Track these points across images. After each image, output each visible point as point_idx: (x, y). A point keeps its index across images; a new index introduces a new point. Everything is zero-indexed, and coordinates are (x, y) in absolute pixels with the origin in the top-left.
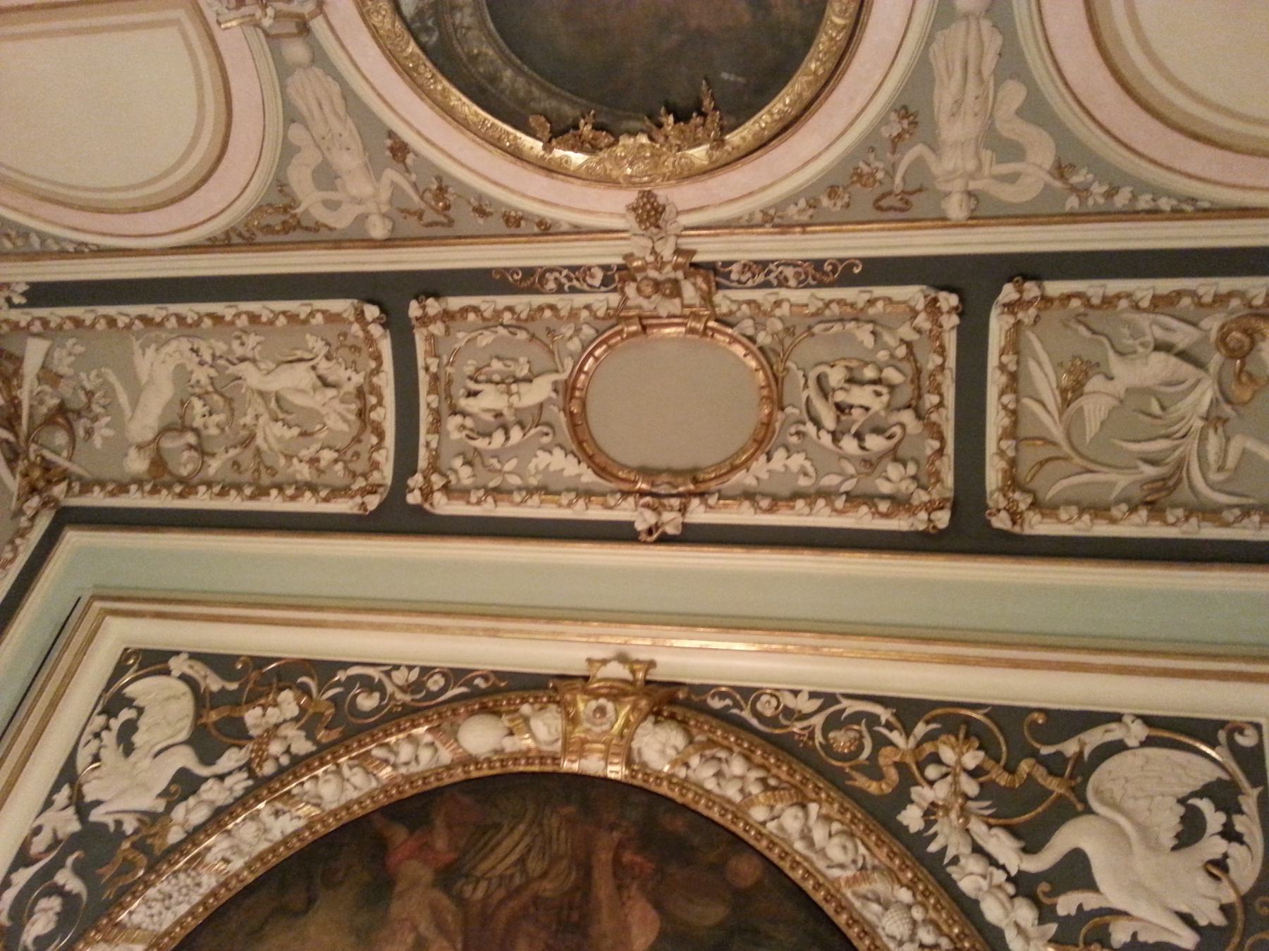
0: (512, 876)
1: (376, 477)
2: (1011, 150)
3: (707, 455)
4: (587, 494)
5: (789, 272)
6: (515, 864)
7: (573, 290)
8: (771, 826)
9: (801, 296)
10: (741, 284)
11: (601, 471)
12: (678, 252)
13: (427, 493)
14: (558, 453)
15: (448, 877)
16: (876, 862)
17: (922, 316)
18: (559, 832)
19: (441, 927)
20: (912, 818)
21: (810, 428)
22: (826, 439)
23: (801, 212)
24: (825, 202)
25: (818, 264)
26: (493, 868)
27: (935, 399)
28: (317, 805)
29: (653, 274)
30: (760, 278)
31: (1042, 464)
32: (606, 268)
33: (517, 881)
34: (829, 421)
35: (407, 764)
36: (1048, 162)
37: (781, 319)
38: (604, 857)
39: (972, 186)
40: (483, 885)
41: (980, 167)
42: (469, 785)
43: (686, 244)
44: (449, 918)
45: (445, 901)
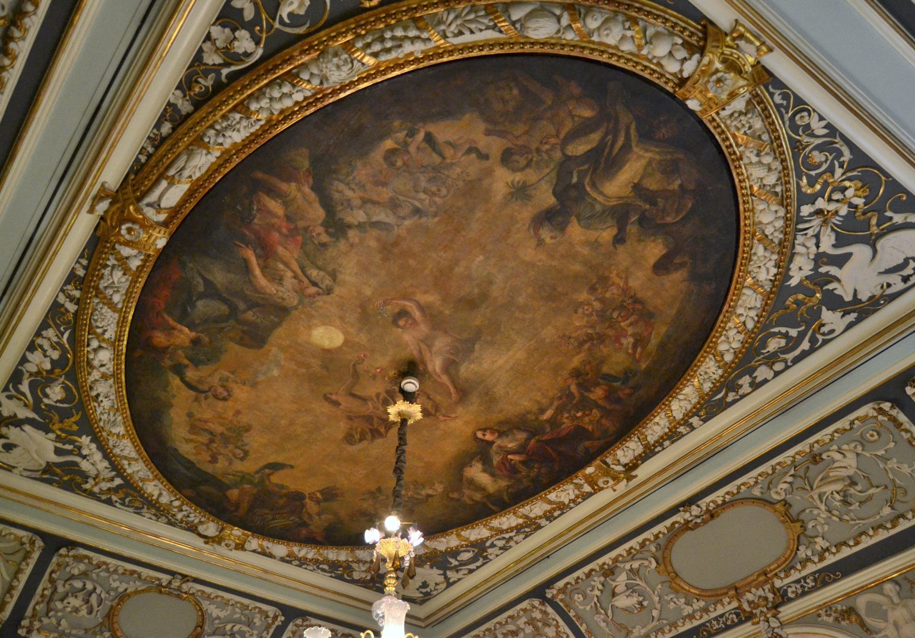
1: (295, 628)
3: (154, 595)
4: (208, 597)
8: (173, 499)
11: (198, 603)
13: (275, 617)
17: (36, 628)
20: (118, 481)
21: (103, 596)
22: (98, 591)
27: (46, 592)
31: (13, 554)
34: (94, 599)
42: (289, 540)
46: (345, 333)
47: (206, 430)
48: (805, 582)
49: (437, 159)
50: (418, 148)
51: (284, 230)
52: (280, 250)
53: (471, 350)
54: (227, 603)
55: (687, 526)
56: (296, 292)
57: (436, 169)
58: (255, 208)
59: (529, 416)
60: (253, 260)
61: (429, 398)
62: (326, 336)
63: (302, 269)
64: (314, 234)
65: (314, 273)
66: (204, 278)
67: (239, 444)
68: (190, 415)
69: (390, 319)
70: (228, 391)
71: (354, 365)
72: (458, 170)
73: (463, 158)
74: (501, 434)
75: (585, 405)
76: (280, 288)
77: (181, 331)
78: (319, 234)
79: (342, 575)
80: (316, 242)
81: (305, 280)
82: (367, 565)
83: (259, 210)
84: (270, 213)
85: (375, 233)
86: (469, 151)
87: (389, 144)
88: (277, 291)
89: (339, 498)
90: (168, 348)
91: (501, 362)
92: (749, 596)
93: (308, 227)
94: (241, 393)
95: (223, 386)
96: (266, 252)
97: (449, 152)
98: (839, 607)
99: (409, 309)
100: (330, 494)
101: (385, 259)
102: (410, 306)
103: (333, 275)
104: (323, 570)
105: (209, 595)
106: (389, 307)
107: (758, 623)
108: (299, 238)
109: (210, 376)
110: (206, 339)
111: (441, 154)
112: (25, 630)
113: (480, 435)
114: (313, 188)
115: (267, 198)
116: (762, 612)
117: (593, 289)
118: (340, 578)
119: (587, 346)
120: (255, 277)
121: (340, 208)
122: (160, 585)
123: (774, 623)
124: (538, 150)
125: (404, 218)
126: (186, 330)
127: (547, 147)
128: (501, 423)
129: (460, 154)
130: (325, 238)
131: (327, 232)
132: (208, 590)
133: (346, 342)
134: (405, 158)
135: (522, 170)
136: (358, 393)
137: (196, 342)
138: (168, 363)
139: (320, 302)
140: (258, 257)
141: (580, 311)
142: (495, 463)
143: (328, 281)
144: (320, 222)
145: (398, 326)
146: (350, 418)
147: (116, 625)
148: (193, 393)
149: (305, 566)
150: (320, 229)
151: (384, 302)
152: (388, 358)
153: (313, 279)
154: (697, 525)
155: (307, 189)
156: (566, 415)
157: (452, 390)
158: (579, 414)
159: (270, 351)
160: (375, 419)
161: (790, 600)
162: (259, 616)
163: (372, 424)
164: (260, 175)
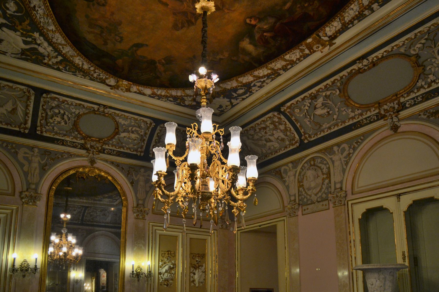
2: (26, 158)
5: (69, 144)
7: (111, 150)
9: (67, 139)
10: (79, 143)
12: (89, 153)
13: (151, 124)
14: (122, 124)
23: (64, 155)
24: (60, 156)
25: (63, 144)
29: (95, 151)
30: (75, 144)
32: (104, 153)
36: (19, 154)
37: (72, 136)
39: (33, 153)
41: (32, 157)
43: (87, 154)
48: (417, 99)
54: (127, 118)
55: (359, 71)
74: (260, 20)
79: (180, 103)
82: (192, 98)
92: (385, 107)
98: (432, 111)
104: (170, 101)
105: (118, 114)
107: (387, 120)
112: (40, 132)
113: (248, 21)
116: (390, 114)
118: (179, 104)
122: (94, 110)
123: (395, 119)
132: (117, 112)
142: (256, 38)
147: (79, 129)
149: (161, 99)
154: (365, 70)
156: (299, 6)
158: (306, 5)
161: (407, 108)
162: (143, 123)
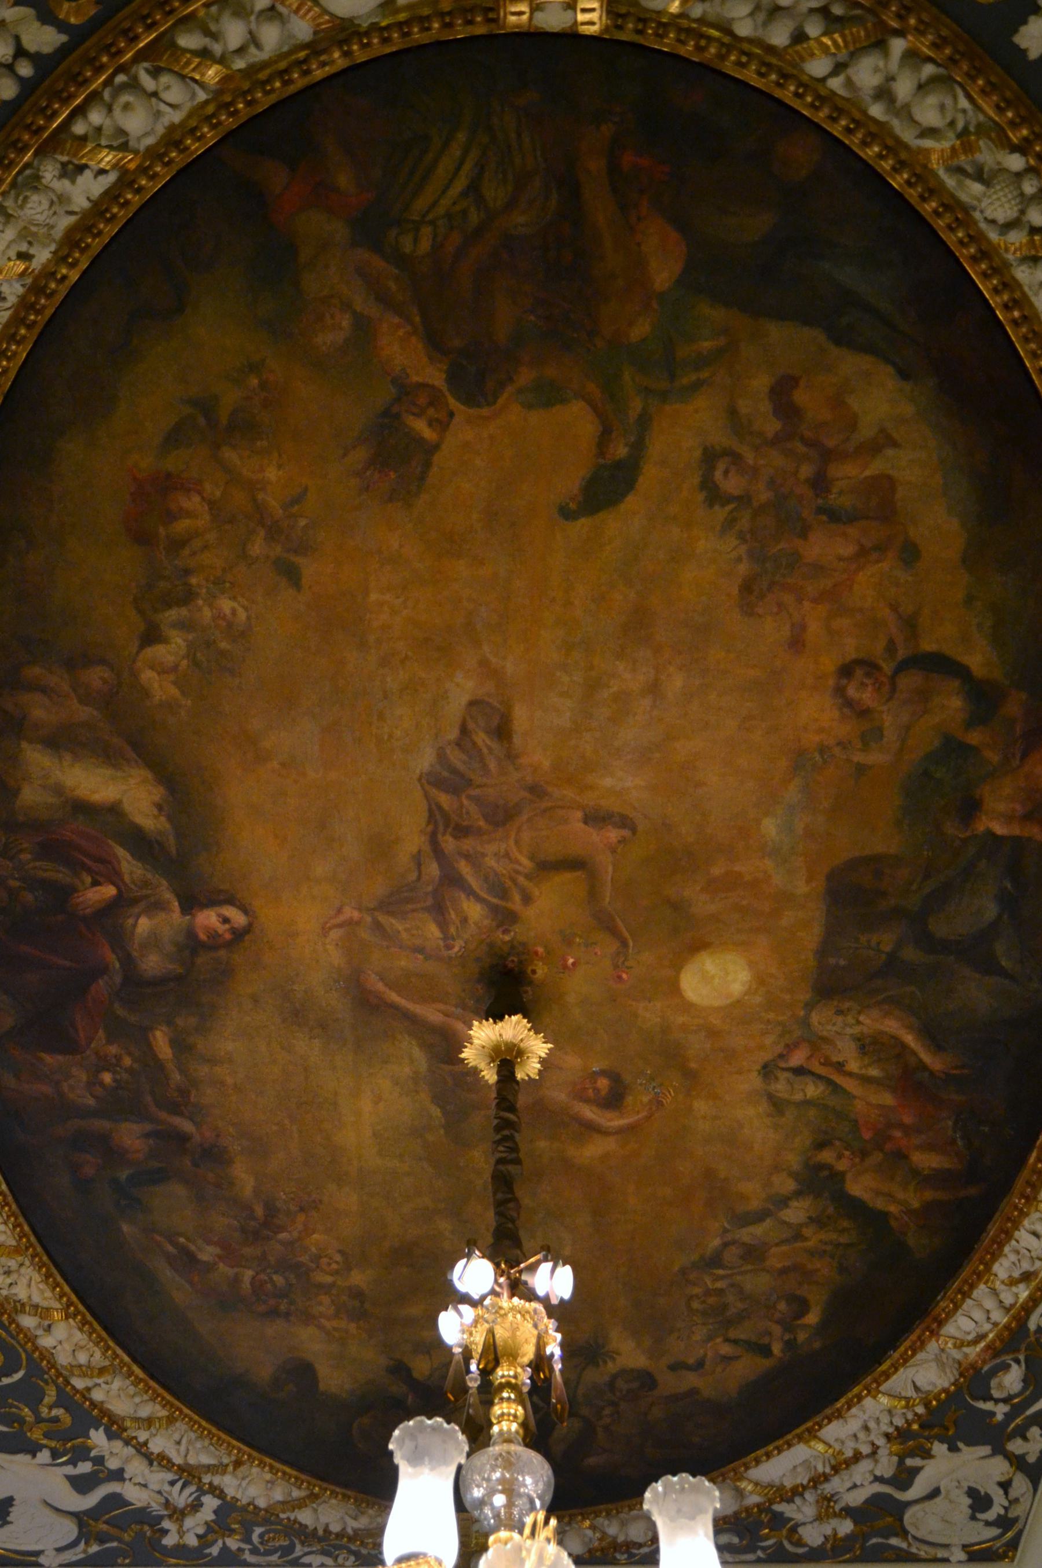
0: (464, 212)
6: (464, 194)
15: (372, 227)
16: (981, 118)
18: (519, 135)
19: (384, 299)
26: (434, 204)
28: (124, 147)
33: (474, 218)
35: (241, 51)
38: (595, 165)
40: (426, 231)
44: (392, 285)
45: (378, 263)
46: (688, 1007)
47: (852, 518)
49: (732, 1334)
50: (770, 1334)
51: (898, 1134)
52: (888, 1099)
53: (438, 1099)
56: (825, 1040)
57: (729, 1323)
58: (960, 1143)
59: (193, 1021)
60: (926, 1057)
61: (419, 950)
62: (717, 980)
63: (835, 1087)
64: (847, 1153)
65: (812, 1090)
66: (1002, 972)
67: (744, 522)
68: (910, 554)
69: (627, 1078)
70: (849, 703)
71: (624, 943)
72: (697, 1337)
73: (702, 1351)
75: (121, 1104)
76: (856, 1030)
77: (1009, 818)
78: (840, 1157)
80: (837, 1143)
81: (822, 1071)
83: (953, 1142)
84: (929, 1147)
85: (755, 1204)
86: (700, 1364)
87: (812, 1318)
88: (859, 1022)
89: (360, 455)
90: (1024, 756)
91: (366, 1105)
93: (862, 1160)
94: (816, 715)
95: (864, 713)
96: (909, 1080)
97: (726, 1349)
99: (609, 1114)
100: (396, 458)
101: (709, 1174)
102: (613, 1121)
103: (777, 1106)
106: (645, 1099)
108: (867, 1135)
109: (908, 728)
110: (951, 829)
111: (735, 1342)
114: (885, 1215)
115: (947, 1166)
117: (357, 1294)
119: (259, 1211)
120: (910, 1028)
121: (831, 1210)
124: (613, 1404)
125: (726, 1245)
126: (999, 829)
127: (607, 1411)
128: (223, 975)
129: (710, 1354)
130: (827, 1156)
131: (829, 1167)
133: (674, 988)
134: (777, 1315)
135: (614, 1378)
136: (568, 876)
137: (970, 808)
138: (1014, 706)
139: (771, 1045)
140: (923, 1067)
141: (338, 1258)
143: (780, 1087)
144: (849, 1176)
145: (603, 1073)
146: (536, 791)
148: (928, 646)
150: (841, 1166)
151: (660, 1104)
152: (571, 999)
153: (808, 1079)
155: (893, 1209)
157: (394, 997)
159: (809, 881)
160: (482, 823)
163: (477, 800)
164: (972, 1191)
